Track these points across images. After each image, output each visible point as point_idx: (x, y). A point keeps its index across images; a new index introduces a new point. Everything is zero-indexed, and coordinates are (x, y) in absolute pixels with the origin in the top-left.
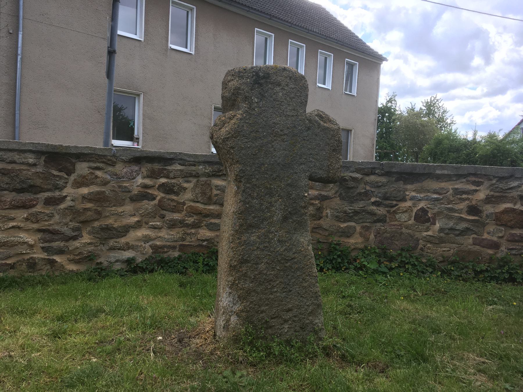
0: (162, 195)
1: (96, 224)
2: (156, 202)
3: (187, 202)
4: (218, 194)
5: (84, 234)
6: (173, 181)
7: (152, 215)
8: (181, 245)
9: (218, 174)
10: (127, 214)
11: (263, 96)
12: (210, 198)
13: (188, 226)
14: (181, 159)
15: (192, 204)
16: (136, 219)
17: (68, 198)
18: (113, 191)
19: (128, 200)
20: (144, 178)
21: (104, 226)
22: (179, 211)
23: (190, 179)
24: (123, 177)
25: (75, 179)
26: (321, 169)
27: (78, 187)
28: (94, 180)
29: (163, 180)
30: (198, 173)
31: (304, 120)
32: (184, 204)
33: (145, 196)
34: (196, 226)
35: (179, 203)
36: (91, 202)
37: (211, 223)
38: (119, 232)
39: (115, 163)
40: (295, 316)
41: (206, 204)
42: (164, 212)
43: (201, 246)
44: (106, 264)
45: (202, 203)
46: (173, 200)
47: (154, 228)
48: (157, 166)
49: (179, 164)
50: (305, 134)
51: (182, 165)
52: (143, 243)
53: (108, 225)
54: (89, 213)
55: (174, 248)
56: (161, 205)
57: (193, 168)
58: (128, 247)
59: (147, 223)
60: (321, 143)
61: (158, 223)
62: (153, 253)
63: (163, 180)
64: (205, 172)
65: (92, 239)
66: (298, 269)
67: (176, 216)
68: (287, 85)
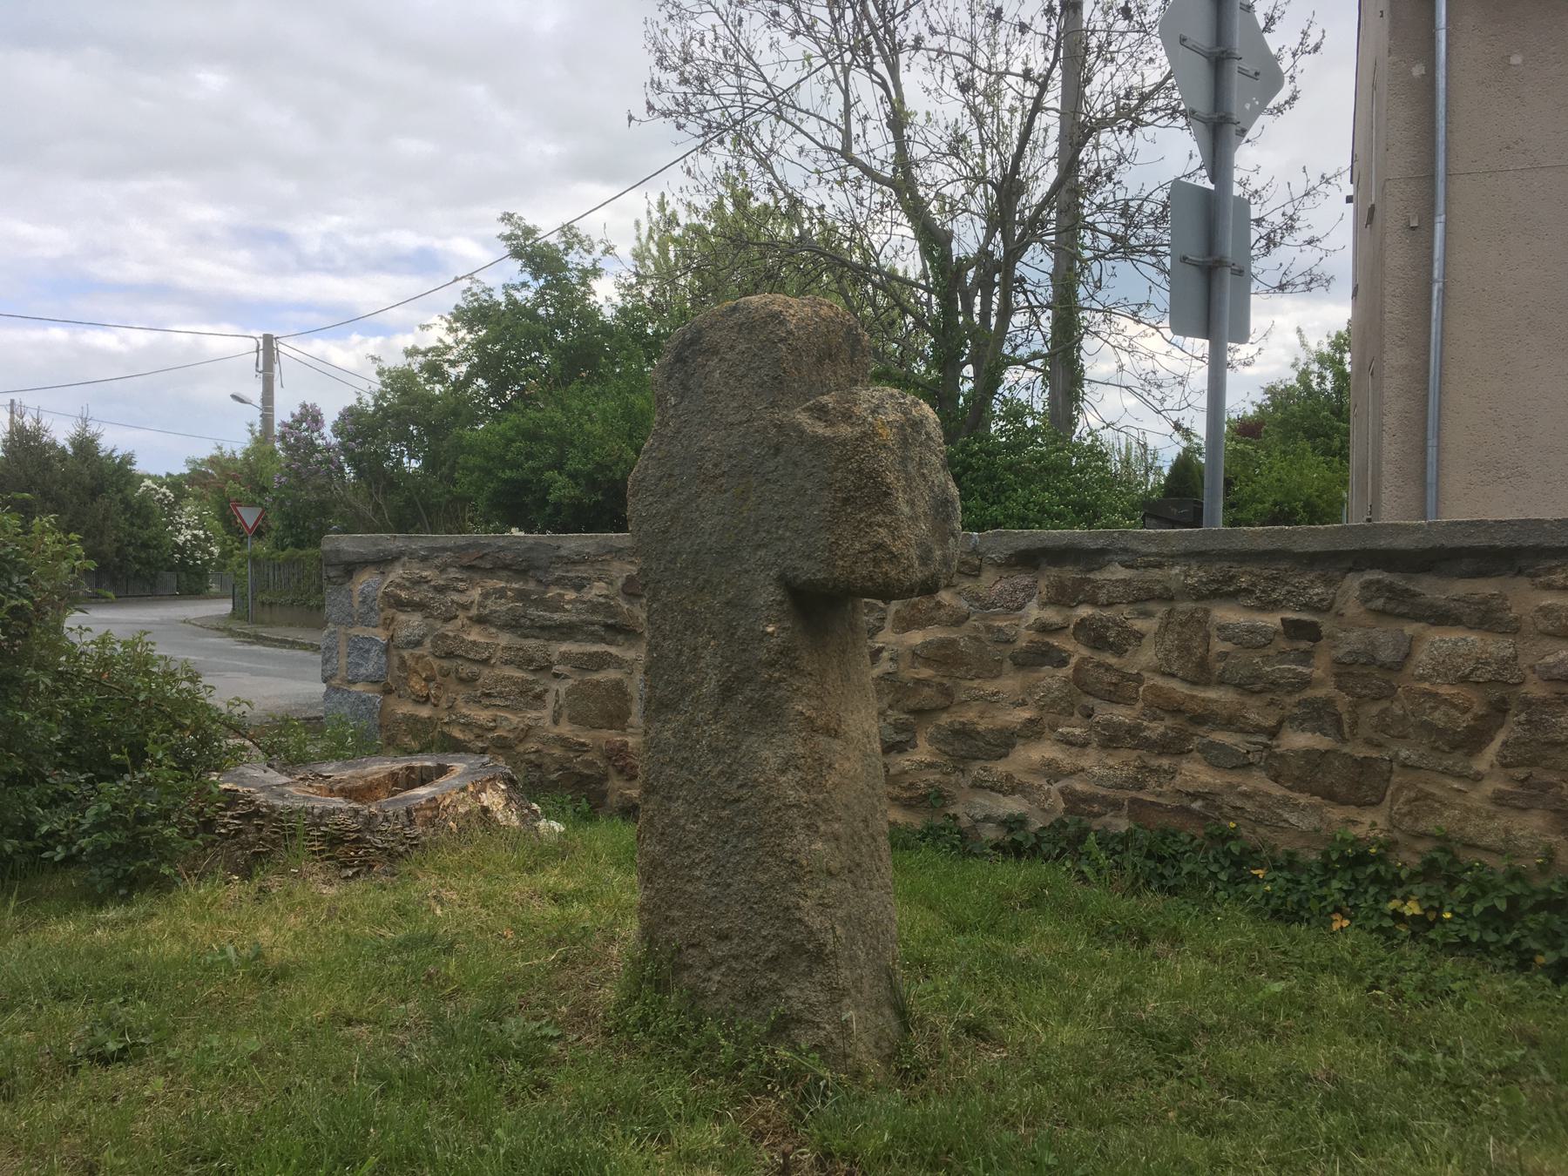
0: (1085, 652)
1: (944, 719)
2: (1068, 671)
3: (1146, 675)
4: (1226, 654)
5: (922, 743)
6: (1107, 613)
7: (1064, 706)
8: (1133, 801)
9: (1226, 589)
10: (1005, 701)
11: (686, 388)
12: (1203, 665)
13: (1148, 744)
14: (1125, 550)
15: (1159, 681)
16: (1027, 715)
17: (885, 654)
18: (976, 638)
19: (1008, 664)
20: (1043, 605)
21: (957, 726)
22: (1129, 701)
23: (1152, 606)
24: (993, 605)
25: (897, 612)
26: (809, 557)
27: (905, 630)
28: (934, 614)
29: (1084, 611)
30: (1167, 589)
31: (765, 428)
32: (1138, 679)
33: (1044, 654)
34: (1173, 747)
35: (1125, 677)
36: (930, 666)
37: (1212, 744)
38: (989, 743)
39: (979, 569)
40: (736, 958)
41: (1194, 683)
42: (1090, 701)
43: (1186, 811)
44: (965, 822)
45: (1184, 680)
46: (1109, 668)
47: (1068, 742)
48: (1070, 573)
49: (1123, 564)
50: (771, 465)
51: (1127, 567)
52: (1044, 782)
53: (964, 724)
54: (927, 691)
55: (1116, 805)
56: (1079, 681)
57: (1156, 574)
58: (1010, 787)
59: (1053, 729)
60: (808, 486)
61: (1077, 731)
62: (1067, 811)
63: (1084, 611)
64: (1186, 586)
65: (934, 755)
66: (747, 831)
67: (1122, 715)
68: (732, 348)
